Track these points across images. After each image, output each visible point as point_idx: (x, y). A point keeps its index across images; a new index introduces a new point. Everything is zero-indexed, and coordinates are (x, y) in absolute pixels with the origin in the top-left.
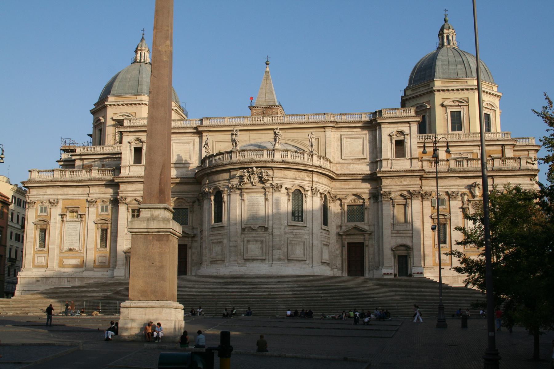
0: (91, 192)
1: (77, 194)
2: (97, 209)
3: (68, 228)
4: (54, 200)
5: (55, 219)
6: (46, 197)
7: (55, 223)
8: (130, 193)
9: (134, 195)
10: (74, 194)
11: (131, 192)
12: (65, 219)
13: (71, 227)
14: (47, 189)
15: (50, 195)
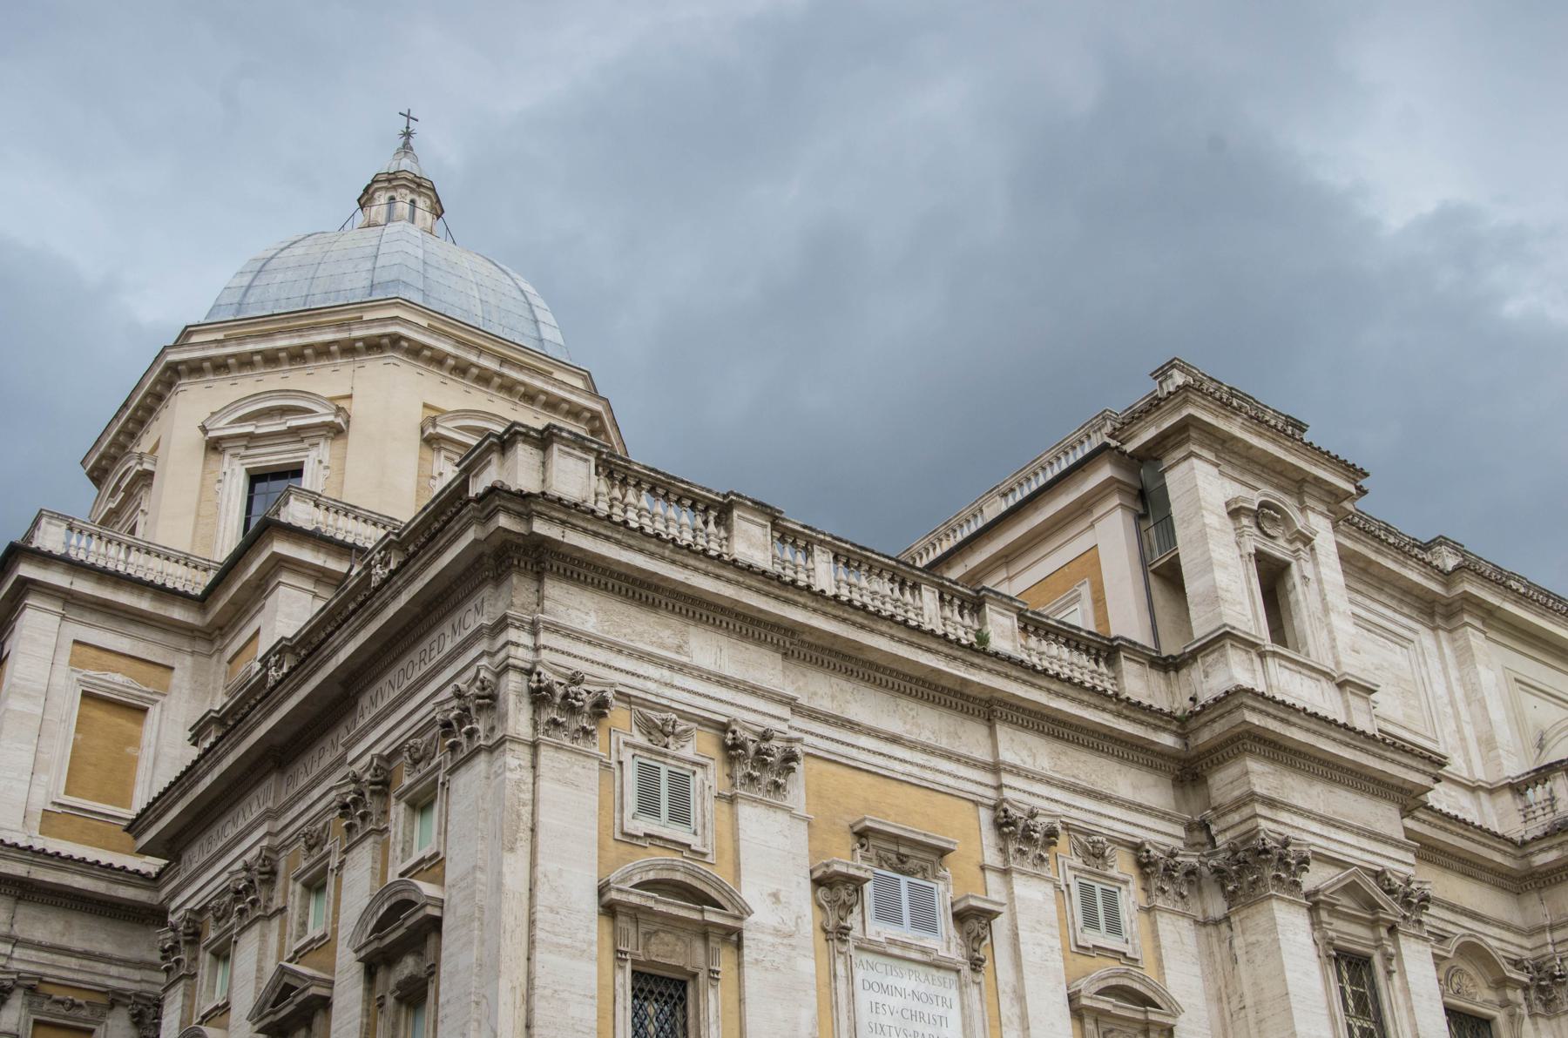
0: (1007, 755)
1: (912, 745)
2: (1061, 891)
3: (875, 1007)
4: (766, 736)
5: (775, 896)
6: (685, 693)
7: (776, 932)
8: (1310, 835)
9: (1334, 850)
10: (894, 739)
11: (1315, 827)
12: (853, 921)
13: (895, 1002)
14: (692, 629)
15: (722, 681)
